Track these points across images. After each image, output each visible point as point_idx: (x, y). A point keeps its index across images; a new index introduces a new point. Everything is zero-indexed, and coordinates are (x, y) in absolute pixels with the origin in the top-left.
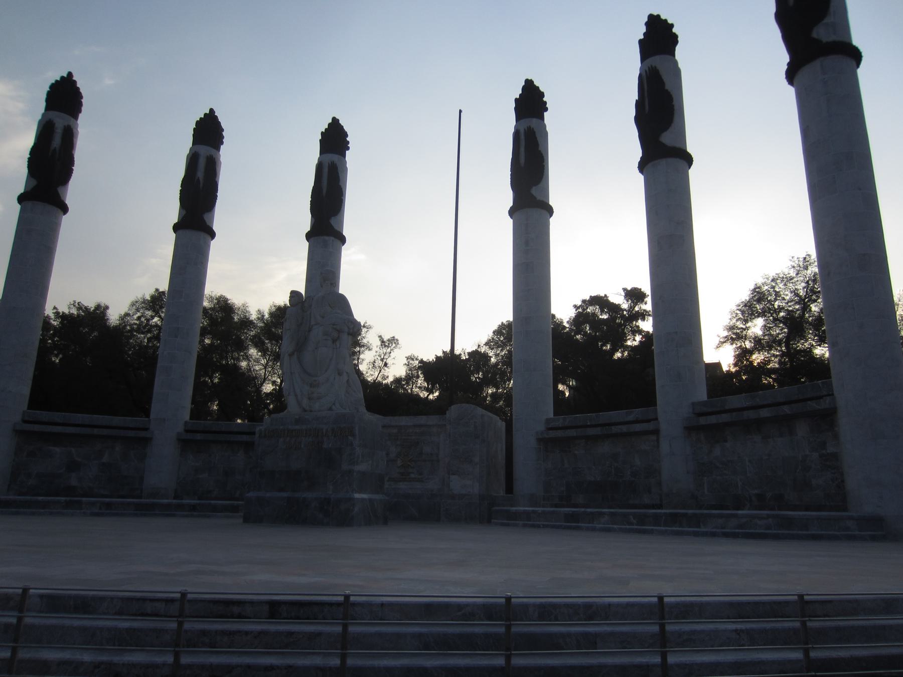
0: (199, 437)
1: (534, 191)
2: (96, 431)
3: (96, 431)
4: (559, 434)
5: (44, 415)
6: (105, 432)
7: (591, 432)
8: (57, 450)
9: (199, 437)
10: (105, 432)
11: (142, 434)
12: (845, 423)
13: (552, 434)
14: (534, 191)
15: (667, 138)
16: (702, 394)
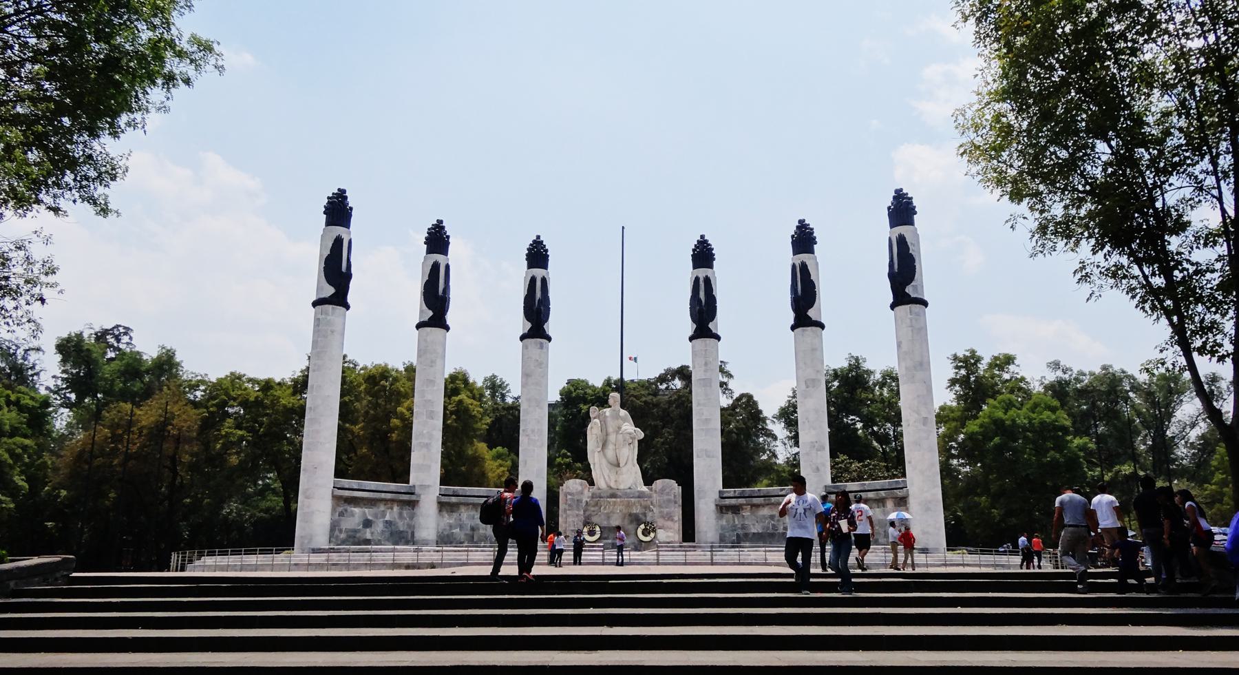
0: (454, 499)
1: (711, 325)
2: (383, 495)
3: (383, 495)
4: (733, 501)
5: (346, 482)
6: (389, 496)
7: (756, 501)
8: (357, 510)
9: (454, 499)
10: (389, 496)
11: (413, 498)
12: (912, 502)
13: (727, 502)
14: (711, 325)
15: (811, 313)
16: (829, 482)
